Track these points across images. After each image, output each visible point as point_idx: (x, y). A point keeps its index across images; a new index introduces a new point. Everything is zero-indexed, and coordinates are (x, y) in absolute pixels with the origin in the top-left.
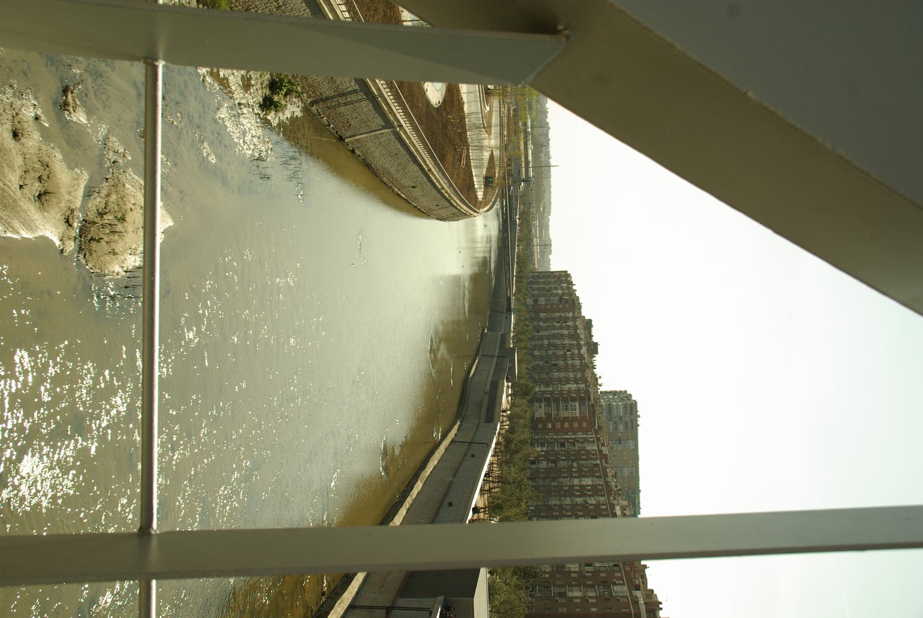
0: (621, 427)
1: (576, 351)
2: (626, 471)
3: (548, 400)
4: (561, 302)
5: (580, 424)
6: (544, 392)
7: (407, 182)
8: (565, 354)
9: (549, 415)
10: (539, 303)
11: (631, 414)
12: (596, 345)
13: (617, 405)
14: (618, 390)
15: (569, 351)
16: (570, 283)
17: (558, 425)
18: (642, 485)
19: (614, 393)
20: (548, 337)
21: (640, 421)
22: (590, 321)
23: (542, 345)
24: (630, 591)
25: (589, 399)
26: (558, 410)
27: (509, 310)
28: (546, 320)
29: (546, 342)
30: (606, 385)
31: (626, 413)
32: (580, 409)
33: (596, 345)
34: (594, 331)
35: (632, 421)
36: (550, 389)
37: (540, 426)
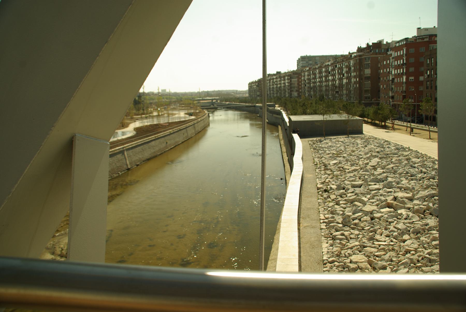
1: (275, 80)
3: (291, 91)
6: (288, 93)
7: (164, 145)
9: (297, 91)
16: (252, 83)
19: (298, 65)
20: (270, 91)
21: (308, 55)
24: (352, 59)
25: (291, 75)
27: (255, 106)
29: (272, 92)
30: (294, 67)
31: (305, 61)
36: (287, 90)
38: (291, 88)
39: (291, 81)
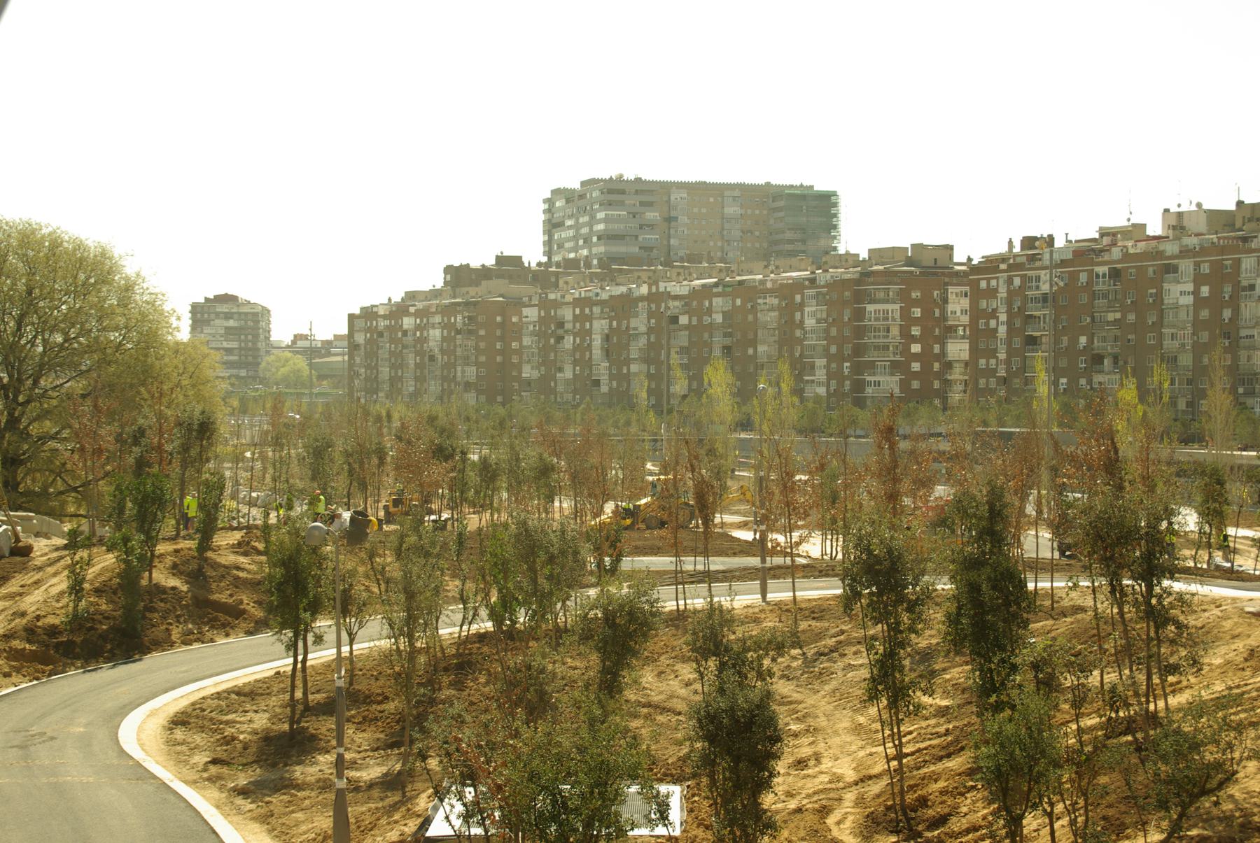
0: (652, 215)
2: (731, 210)
3: (858, 368)
4: (470, 332)
5: (916, 303)
6: (830, 376)
8: (687, 327)
9: (895, 367)
10: (473, 379)
11: (623, 192)
12: (501, 260)
13: (606, 220)
14: (542, 217)
15: (674, 320)
17: (916, 348)
18: (755, 176)
19: (552, 225)
21: (629, 175)
22: (448, 270)
23: (650, 376)
26: (886, 348)
28: (550, 365)
31: (622, 203)
32: (887, 302)
33: (501, 260)
34: (475, 263)
36: (821, 362)
37: (915, 385)
38: (859, 350)
39: (859, 314)
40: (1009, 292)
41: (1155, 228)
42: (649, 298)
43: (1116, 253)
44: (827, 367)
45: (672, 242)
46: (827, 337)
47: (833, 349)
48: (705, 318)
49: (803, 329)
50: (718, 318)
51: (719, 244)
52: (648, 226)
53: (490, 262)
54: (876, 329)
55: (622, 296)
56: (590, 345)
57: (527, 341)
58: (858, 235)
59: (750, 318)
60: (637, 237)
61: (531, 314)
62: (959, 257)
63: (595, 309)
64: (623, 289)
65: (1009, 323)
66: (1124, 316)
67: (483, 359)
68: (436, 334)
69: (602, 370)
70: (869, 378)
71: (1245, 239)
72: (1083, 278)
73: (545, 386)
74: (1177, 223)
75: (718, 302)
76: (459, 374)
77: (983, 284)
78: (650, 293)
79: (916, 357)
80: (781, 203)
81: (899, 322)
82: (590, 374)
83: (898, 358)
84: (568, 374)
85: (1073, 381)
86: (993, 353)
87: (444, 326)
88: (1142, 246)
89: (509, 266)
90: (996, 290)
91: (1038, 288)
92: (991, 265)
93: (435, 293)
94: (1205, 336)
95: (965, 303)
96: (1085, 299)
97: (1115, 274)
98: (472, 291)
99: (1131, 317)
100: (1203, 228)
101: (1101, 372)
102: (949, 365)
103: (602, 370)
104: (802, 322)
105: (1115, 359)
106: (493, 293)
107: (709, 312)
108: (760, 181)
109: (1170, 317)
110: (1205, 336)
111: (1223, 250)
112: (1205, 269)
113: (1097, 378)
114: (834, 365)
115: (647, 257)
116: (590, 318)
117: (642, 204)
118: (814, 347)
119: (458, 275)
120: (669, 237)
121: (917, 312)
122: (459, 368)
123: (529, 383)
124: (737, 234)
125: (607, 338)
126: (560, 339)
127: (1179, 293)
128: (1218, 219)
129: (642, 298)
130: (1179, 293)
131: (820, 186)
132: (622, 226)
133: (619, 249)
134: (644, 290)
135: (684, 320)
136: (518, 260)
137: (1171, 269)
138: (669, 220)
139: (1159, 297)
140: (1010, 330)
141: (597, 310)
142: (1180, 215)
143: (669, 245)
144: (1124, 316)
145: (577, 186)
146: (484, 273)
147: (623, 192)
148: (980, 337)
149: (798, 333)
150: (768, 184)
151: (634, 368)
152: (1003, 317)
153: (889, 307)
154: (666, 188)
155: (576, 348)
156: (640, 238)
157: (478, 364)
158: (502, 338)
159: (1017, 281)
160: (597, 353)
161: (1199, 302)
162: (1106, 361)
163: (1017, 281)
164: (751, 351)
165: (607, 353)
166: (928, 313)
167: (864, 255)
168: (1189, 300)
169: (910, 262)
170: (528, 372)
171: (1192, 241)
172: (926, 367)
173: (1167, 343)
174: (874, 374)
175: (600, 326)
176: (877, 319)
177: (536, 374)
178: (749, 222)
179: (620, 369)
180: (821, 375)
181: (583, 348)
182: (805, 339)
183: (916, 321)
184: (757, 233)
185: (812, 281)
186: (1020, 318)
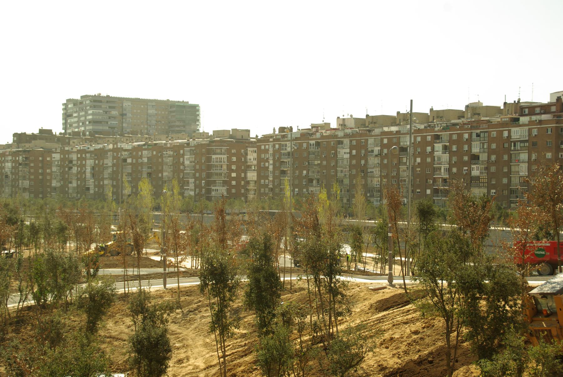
0: (114, 113)
3: (208, 183)
4: (26, 164)
5: (234, 155)
6: (196, 186)
8: (131, 164)
9: (225, 183)
10: (27, 187)
11: (101, 102)
12: (41, 131)
13: (93, 114)
14: (62, 112)
15: (125, 160)
17: (234, 175)
19: (67, 116)
21: (104, 94)
22: (15, 135)
23: (113, 186)
26: (221, 174)
28: (65, 179)
31: (100, 107)
32: (221, 154)
33: (41, 131)
34: (29, 132)
35: (107, 102)
36: (192, 180)
37: (234, 191)
39: (209, 159)
40: (274, 151)
41: (334, 125)
42: (113, 150)
43: (318, 135)
44: (195, 183)
45: (124, 125)
46: (195, 169)
47: (197, 175)
48: (139, 160)
49: (184, 165)
50: (145, 160)
51: (146, 126)
52: (113, 117)
53: (36, 132)
54: (216, 166)
55: (100, 149)
56: (85, 172)
57: (54, 169)
58: (208, 124)
59: (160, 160)
60: (107, 122)
61: (57, 156)
62: (252, 135)
63: (87, 155)
64: (101, 146)
65: (274, 164)
66: (321, 162)
67: (32, 177)
68: (9, 165)
69: (91, 183)
70: (213, 188)
71: (369, 131)
72: (305, 145)
73: (63, 190)
74: (343, 123)
75: (145, 152)
76: (20, 184)
77: (263, 147)
78: (113, 148)
79: (234, 179)
80: (174, 109)
81: (226, 163)
82: (85, 185)
83: (226, 179)
84: (74, 185)
85: (301, 190)
86: (267, 177)
87: (13, 161)
88: (328, 132)
89: (45, 134)
90: (268, 150)
91: (286, 149)
92: (266, 139)
93: (8, 146)
94: (354, 172)
95: (255, 155)
96: (305, 154)
97: (318, 144)
98: (27, 145)
99: (325, 163)
100: (353, 125)
101: (312, 186)
102: (248, 183)
103: (91, 183)
104: (183, 162)
105: (318, 180)
106: (38, 146)
107: (141, 157)
108: (165, 99)
109: (340, 163)
110: (354, 172)
111: (361, 135)
112: (354, 143)
113: (311, 189)
114: (197, 182)
115: (112, 131)
116: (85, 159)
117: (110, 107)
118: (188, 174)
119: (20, 138)
120: (123, 123)
121: (234, 159)
122: (20, 182)
123: (55, 188)
124: (154, 122)
125: (93, 168)
126: (70, 168)
127: (344, 153)
128: (359, 122)
129: (110, 150)
130: (344, 153)
131: (191, 102)
132: (100, 117)
133: (100, 128)
134: (111, 146)
135: (129, 161)
136: (50, 131)
137: (341, 143)
138: (123, 115)
139: (336, 154)
140: (274, 168)
141: (88, 155)
142: (344, 119)
143: (122, 127)
144: (321, 162)
145: (79, 98)
146: (33, 137)
147: (101, 102)
148: (261, 170)
149: (182, 167)
150: (168, 100)
151: (106, 182)
152: (271, 162)
153: (222, 156)
154: (121, 100)
155: (78, 173)
156: (109, 123)
157: (30, 180)
158: (42, 168)
159: (277, 146)
160: (88, 175)
161: (352, 157)
162: (314, 182)
163: (277, 146)
164: (160, 175)
165: (93, 175)
166: (239, 159)
167: (211, 133)
168: (347, 156)
169: (231, 137)
170: (54, 184)
171: (349, 131)
172: (238, 183)
173: (339, 174)
174: (215, 186)
175: (90, 163)
176: (217, 162)
177: (58, 185)
178: (159, 117)
179: (99, 183)
180: (192, 186)
181: (82, 173)
182: (185, 170)
183: (234, 163)
184: (163, 122)
185: (188, 144)
186: (279, 163)
